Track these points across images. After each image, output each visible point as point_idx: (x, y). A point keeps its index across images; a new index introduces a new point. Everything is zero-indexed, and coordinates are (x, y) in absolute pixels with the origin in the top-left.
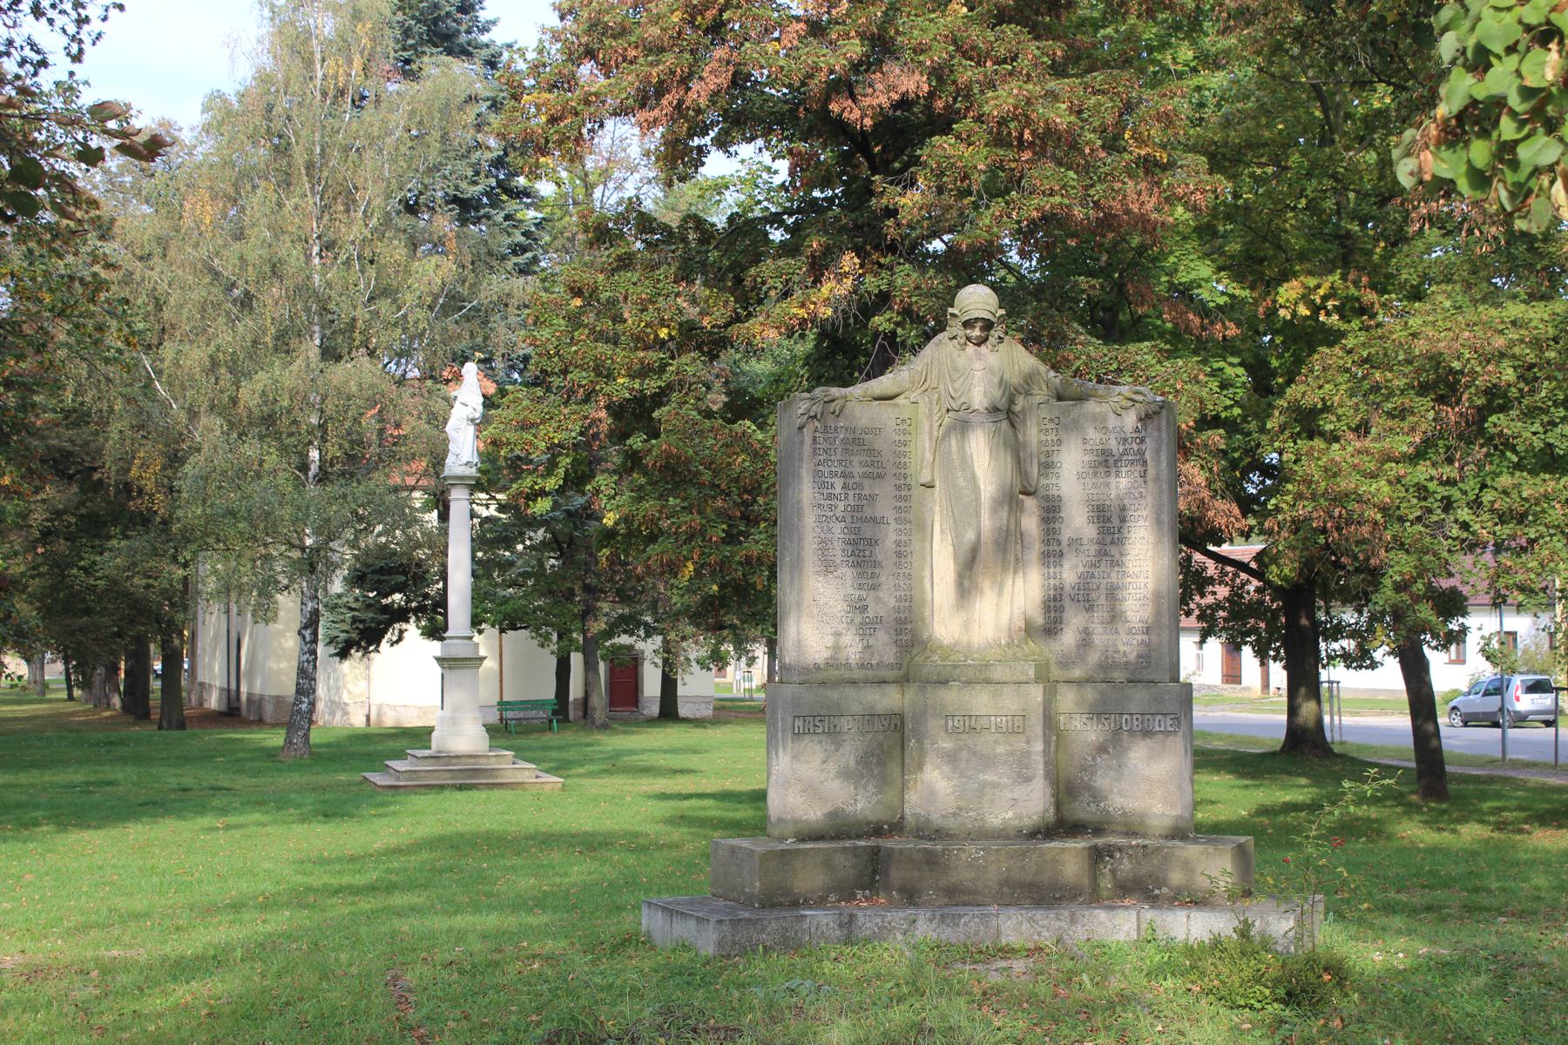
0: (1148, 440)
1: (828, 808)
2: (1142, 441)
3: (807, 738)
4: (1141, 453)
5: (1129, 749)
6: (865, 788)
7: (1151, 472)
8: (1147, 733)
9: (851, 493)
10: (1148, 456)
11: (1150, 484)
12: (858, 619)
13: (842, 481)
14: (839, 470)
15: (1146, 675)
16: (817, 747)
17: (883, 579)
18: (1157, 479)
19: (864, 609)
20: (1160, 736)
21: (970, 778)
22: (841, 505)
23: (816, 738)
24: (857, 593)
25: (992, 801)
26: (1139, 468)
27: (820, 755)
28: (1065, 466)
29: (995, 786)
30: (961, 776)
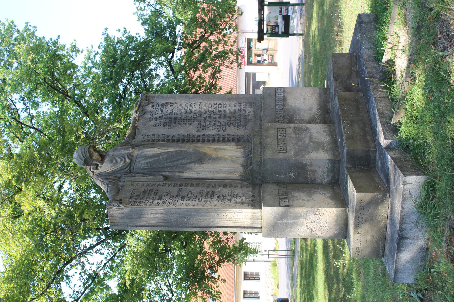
0: (157, 102)
2: (158, 104)
4: (163, 105)
5: (291, 106)
7: (172, 101)
8: (284, 99)
10: (164, 102)
11: (176, 101)
15: (259, 104)
17: (209, 190)
18: (174, 98)
20: (285, 94)
21: (308, 146)
25: (318, 139)
26: (169, 106)
28: (164, 133)
29: (311, 138)
30: (307, 148)
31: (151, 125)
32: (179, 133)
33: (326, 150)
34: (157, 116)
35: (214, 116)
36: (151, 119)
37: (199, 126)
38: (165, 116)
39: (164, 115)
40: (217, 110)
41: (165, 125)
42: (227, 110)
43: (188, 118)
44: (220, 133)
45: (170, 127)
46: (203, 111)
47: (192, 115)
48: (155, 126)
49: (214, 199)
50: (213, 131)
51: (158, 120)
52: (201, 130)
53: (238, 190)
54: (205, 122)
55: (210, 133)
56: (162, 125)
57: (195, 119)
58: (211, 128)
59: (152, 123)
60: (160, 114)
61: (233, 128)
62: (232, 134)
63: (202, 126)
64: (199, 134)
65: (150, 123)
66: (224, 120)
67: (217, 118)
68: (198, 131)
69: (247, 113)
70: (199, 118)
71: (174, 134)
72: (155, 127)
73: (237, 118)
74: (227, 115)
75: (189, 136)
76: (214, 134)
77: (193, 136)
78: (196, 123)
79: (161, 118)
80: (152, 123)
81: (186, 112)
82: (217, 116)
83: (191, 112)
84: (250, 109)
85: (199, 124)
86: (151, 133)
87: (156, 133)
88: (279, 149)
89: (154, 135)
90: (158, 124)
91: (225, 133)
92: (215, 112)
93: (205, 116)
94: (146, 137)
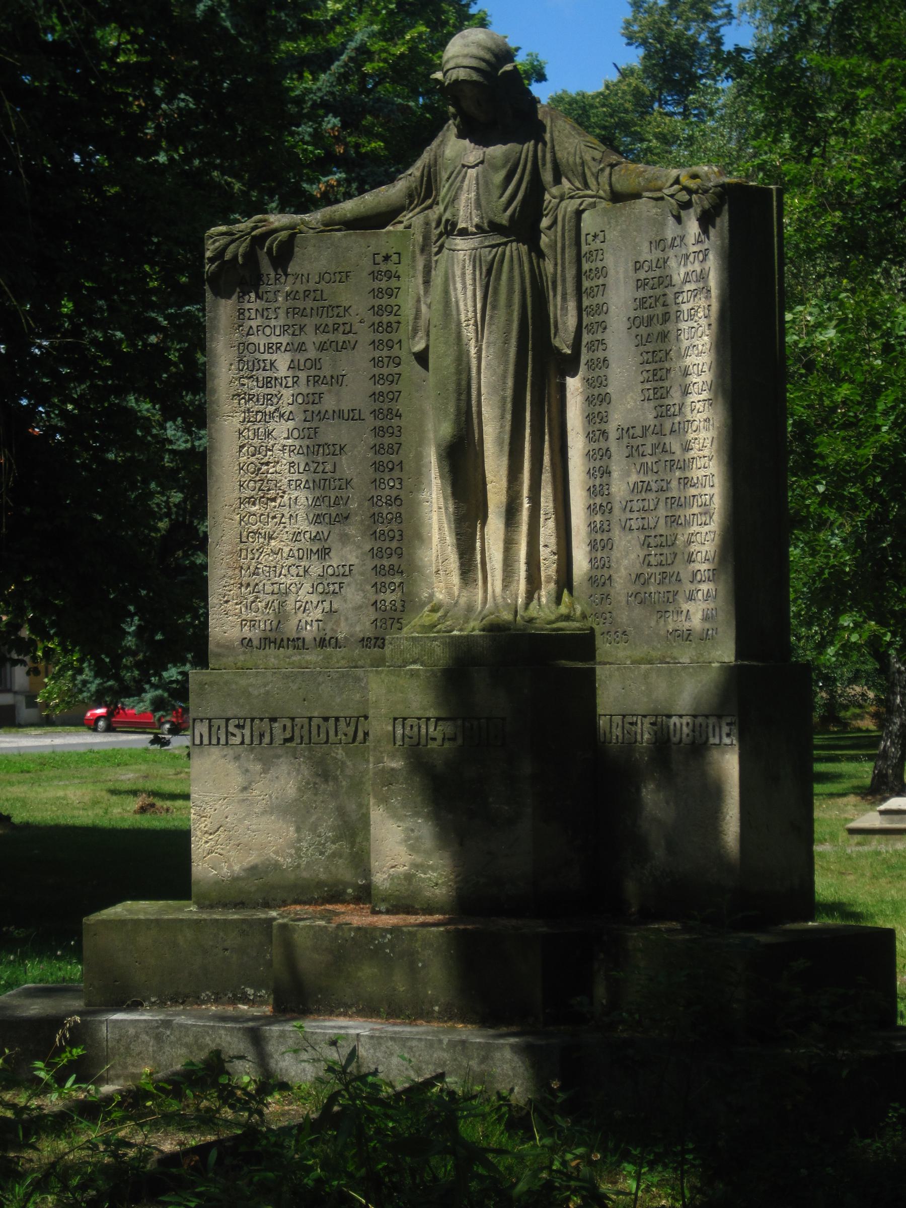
1: (253, 859)
3: (215, 752)
6: (314, 829)
9: (303, 375)
12: (316, 569)
13: (288, 357)
14: (284, 340)
16: (232, 767)
17: (353, 506)
19: (324, 553)
22: (287, 394)
23: (230, 752)
24: (314, 529)
27: (238, 780)
28: (613, 308)
31: (640, 253)
32: (613, 365)
33: (409, 877)
34: (672, 263)
35: (674, 484)
36: (659, 243)
37: (638, 432)
38: (671, 296)
39: (676, 289)
40: (693, 491)
41: (642, 303)
42: (695, 528)
43: (666, 384)
44: (617, 511)
45: (633, 322)
46: (691, 436)
47: (676, 394)
48: (638, 266)
49: (303, 526)
50: (624, 487)
51: (658, 273)
52: (626, 440)
53: (353, 595)
54: (655, 447)
55: (615, 475)
56: (641, 294)
57: (663, 413)
58: (634, 478)
59: (647, 254)
60: (678, 272)
61: (633, 556)
62: (615, 554)
63: (639, 441)
64: (613, 435)
65: (645, 247)
66: (662, 521)
67: (670, 495)
68: (626, 432)
69: (685, 607)
70: (668, 426)
71: (610, 346)
72: (631, 265)
73: (668, 570)
74: (680, 530)
75: (605, 399)
76: (614, 489)
77: (604, 419)
78: (649, 418)
79: (665, 281)
80: (647, 254)
81: (686, 373)
82: (675, 494)
83: (686, 393)
84: (699, 615)
85: (645, 429)
86: (609, 260)
87: (611, 280)
88: (409, 722)
89: (602, 272)
90: (642, 275)
91: (616, 533)
92: (686, 482)
93: (676, 447)
94: (597, 245)
